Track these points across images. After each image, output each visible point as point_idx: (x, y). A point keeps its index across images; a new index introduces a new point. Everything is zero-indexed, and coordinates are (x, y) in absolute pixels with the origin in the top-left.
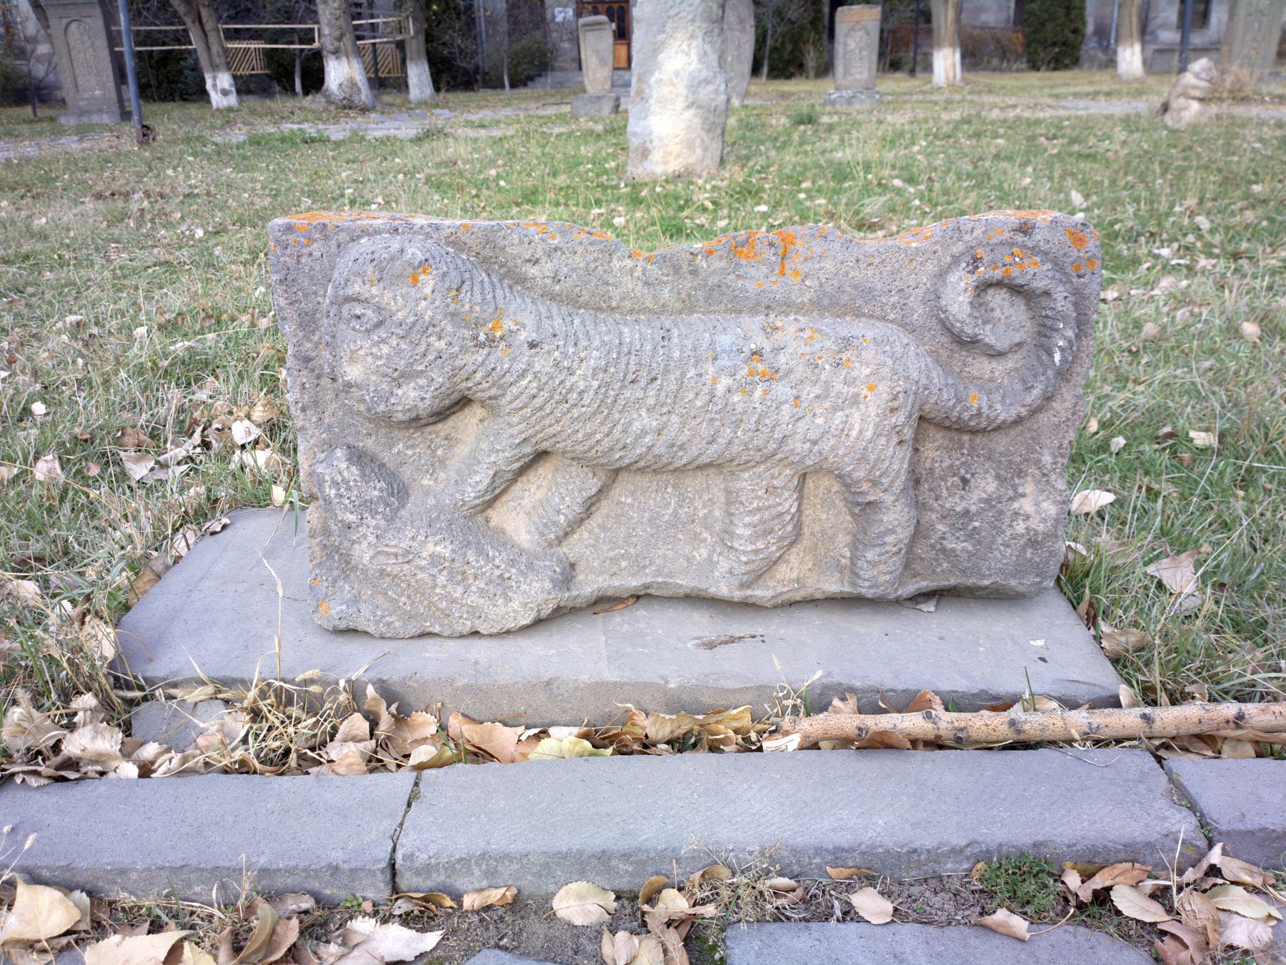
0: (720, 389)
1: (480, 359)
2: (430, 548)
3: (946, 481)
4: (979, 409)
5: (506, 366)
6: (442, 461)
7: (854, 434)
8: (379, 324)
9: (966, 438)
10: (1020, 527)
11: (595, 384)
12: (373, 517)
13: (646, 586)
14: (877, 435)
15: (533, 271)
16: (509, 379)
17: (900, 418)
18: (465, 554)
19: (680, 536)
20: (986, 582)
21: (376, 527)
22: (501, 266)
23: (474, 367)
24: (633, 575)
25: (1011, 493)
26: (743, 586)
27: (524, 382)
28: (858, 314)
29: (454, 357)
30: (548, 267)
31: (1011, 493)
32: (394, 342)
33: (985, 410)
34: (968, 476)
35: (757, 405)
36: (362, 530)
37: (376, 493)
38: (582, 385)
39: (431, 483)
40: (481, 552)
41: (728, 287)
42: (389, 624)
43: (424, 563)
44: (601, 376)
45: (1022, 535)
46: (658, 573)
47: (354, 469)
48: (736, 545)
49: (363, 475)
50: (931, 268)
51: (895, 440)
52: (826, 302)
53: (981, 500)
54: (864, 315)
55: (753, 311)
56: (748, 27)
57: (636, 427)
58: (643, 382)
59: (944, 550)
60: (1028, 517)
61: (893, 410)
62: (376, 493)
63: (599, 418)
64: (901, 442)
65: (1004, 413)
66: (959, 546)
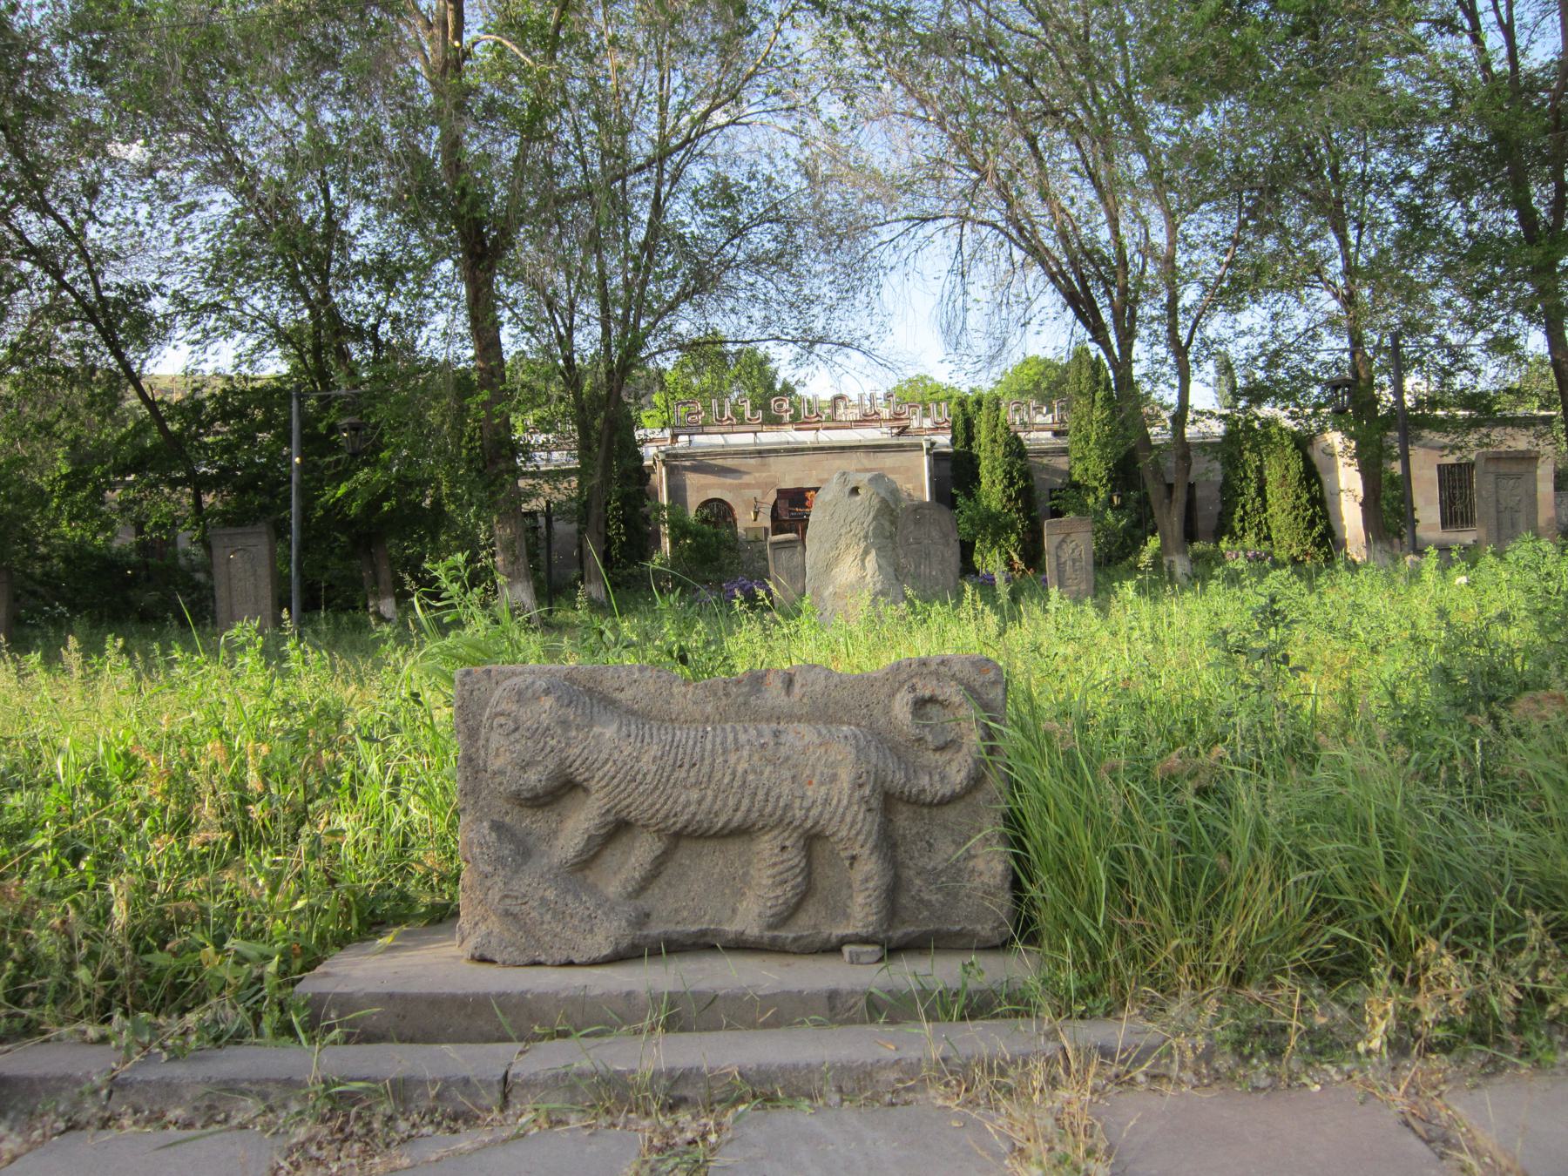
0: (740, 770)
6: (555, 832)
7: (835, 802)
8: (516, 729)
9: (925, 811)
13: (703, 933)
14: (850, 803)
16: (596, 765)
17: (867, 791)
20: (958, 928)
29: (562, 751)
36: (496, 878)
40: (577, 896)
46: (712, 921)
49: (499, 839)
50: (886, 689)
51: (864, 807)
56: (952, 541)
57: (683, 799)
58: (686, 766)
59: (922, 901)
61: (861, 786)
63: (658, 793)
64: (869, 810)
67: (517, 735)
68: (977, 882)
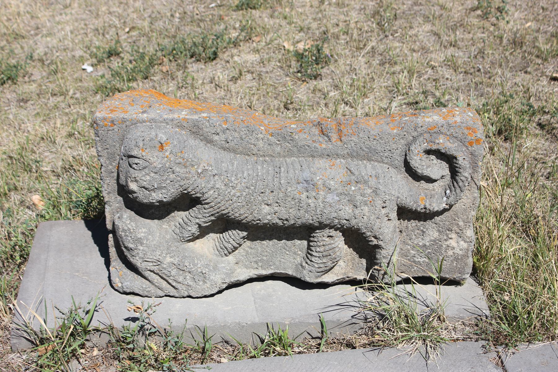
1: (191, 182)
2: (168, 260)
3: (414, 232)
4: (425, 206)
5: (203, 185)
10: (450, 253)
11: (244, 193)
12: (141, 246)
15: (216, 138)
18: (184, 262)
19: (287, 253)
21: (143, 250)
22: (201, 136)
23: (188, 186)
24: (265, 269)
25: (445, 237)
26: (317, 277)
27: (212, 192)
28: (369, 160)
30: (223, 137)
31: (445, 237)
32: (152, 174)
33: (428, 207)
34: (425, 230)
35: (321, 204)
37: (143, 234)
38: (238, 194)
39: (167, 227)
41: (309, 146)
42: (149, 291)
43: (165, 266)
44: (247, 190)
45: (451, 256)
47: (132, 223)
48: (313, 260)
52: (355, 154)
53: (431, 241)
54: (373, 160)
55: (321, 156)
59: (414, 262)
60: (453, 248)
62: (143, 234)
65: (436, 207)
66: (422, 260)
67: (146, 170)
68: (450, 253)
